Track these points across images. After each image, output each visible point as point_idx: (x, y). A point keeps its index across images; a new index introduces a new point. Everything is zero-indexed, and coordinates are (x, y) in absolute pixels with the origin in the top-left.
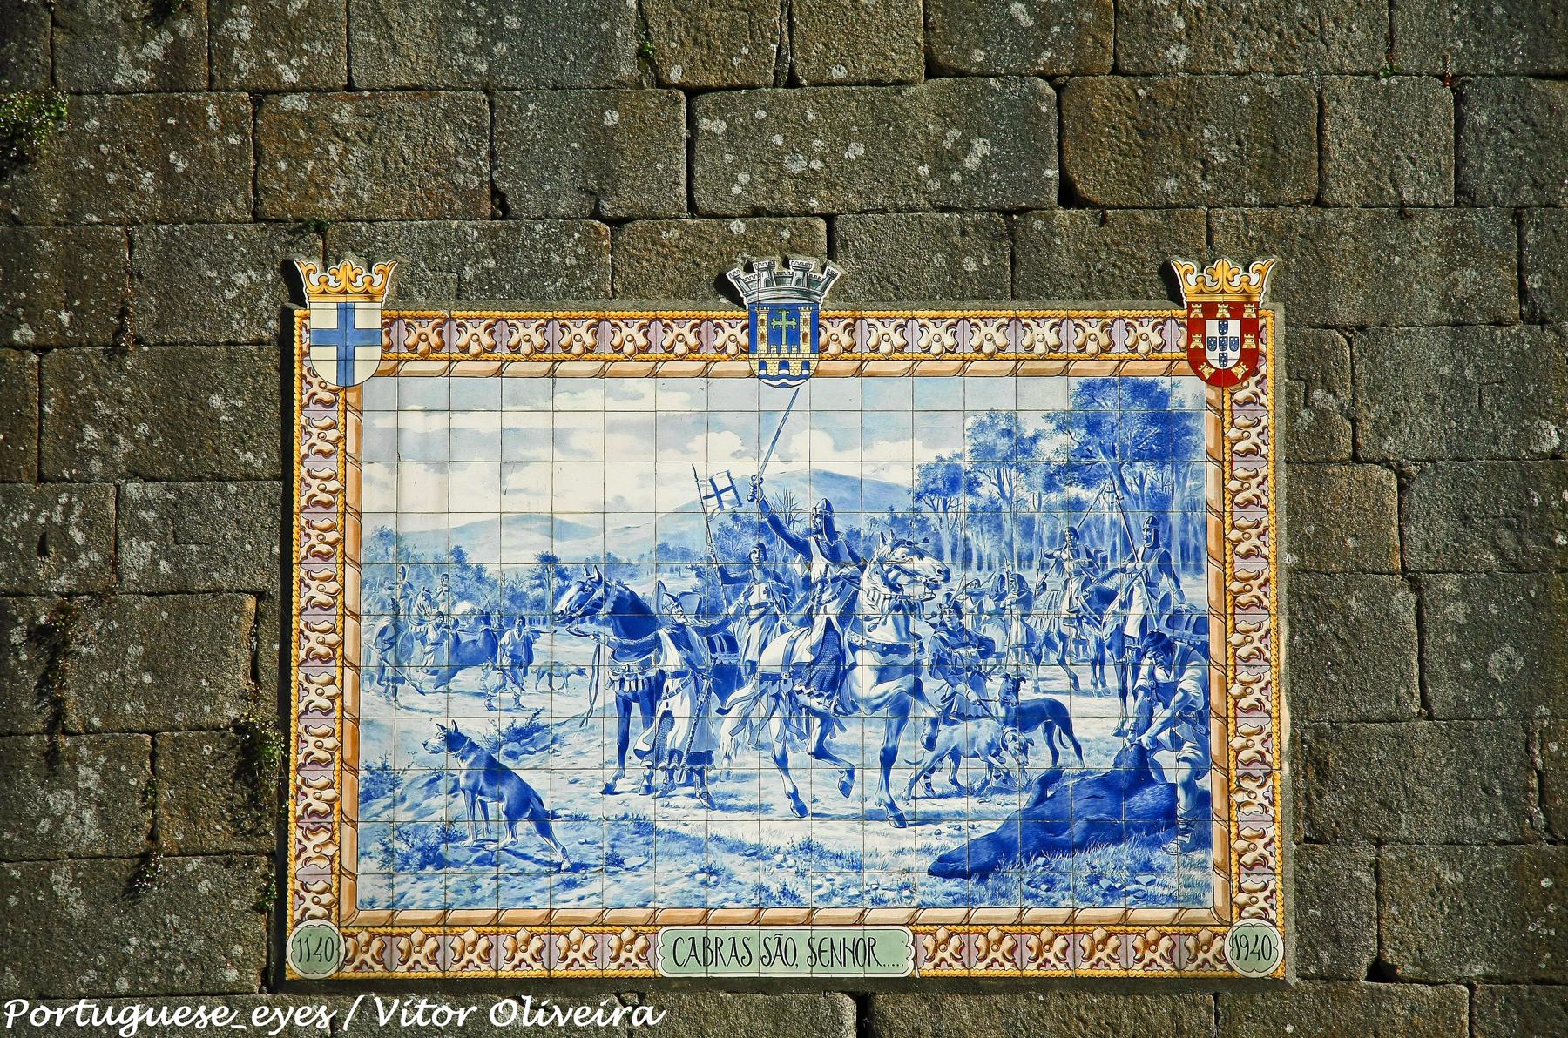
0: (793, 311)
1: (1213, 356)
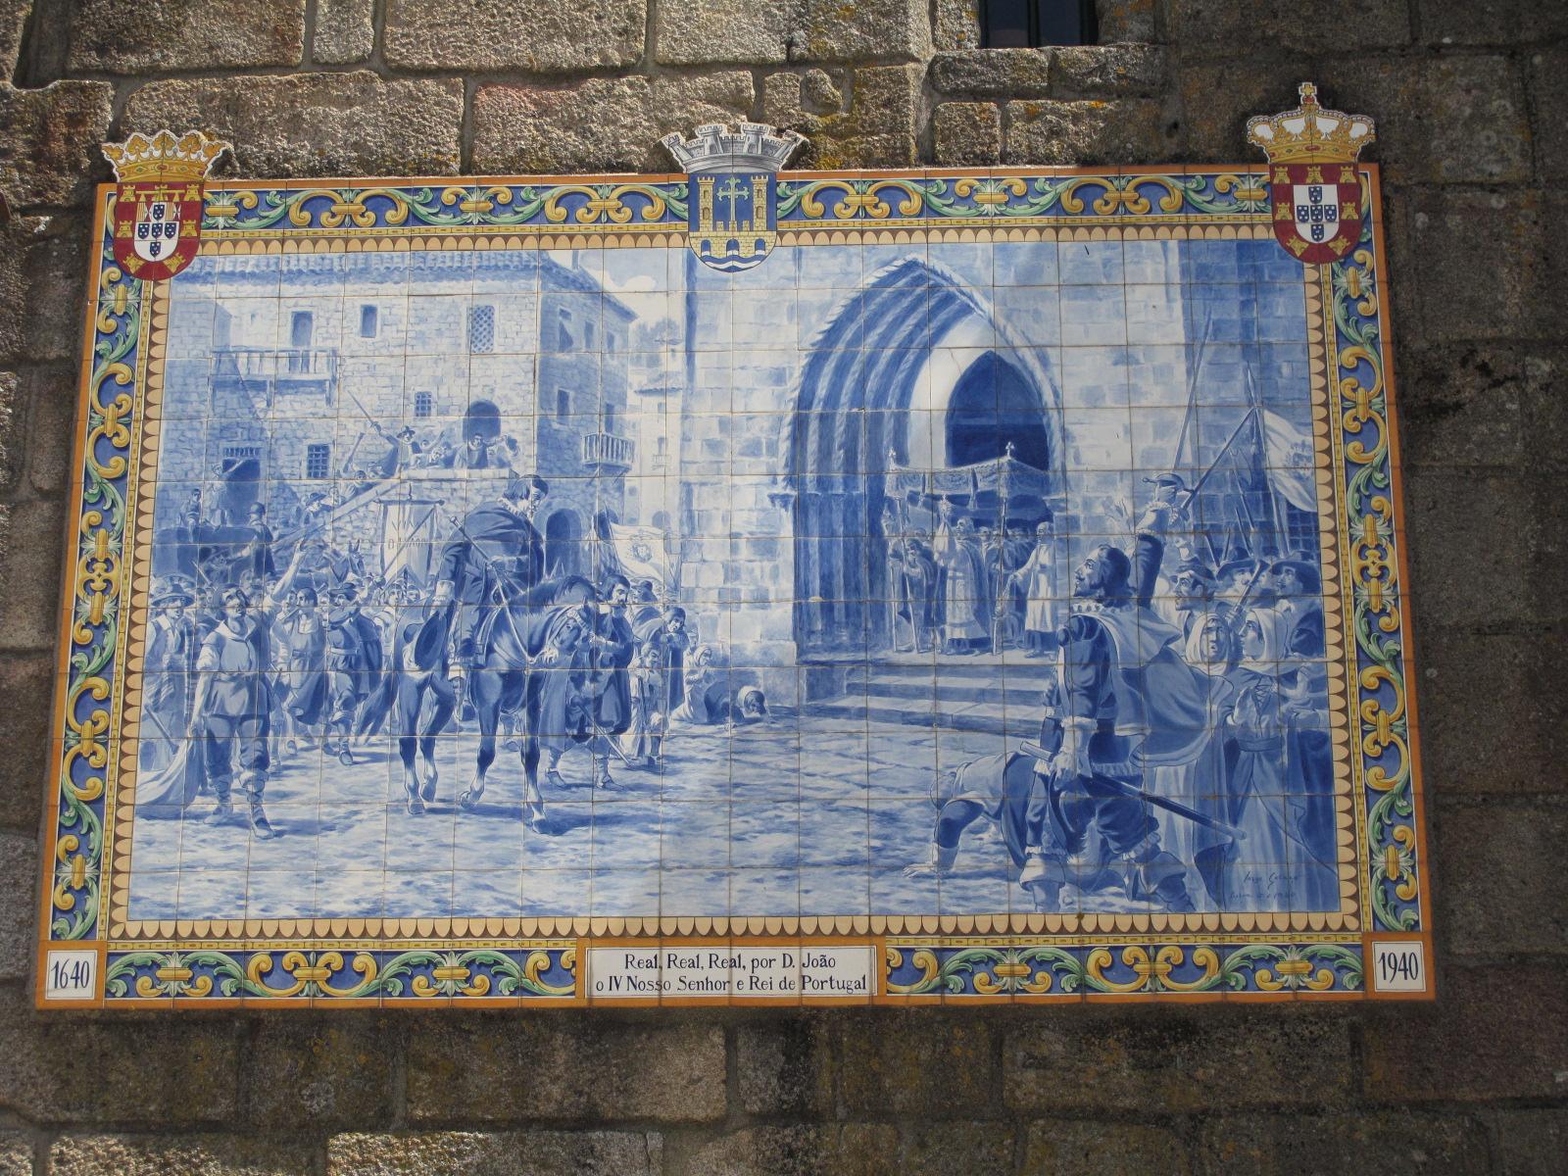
0: (745, 180)
1: (1305, 230)
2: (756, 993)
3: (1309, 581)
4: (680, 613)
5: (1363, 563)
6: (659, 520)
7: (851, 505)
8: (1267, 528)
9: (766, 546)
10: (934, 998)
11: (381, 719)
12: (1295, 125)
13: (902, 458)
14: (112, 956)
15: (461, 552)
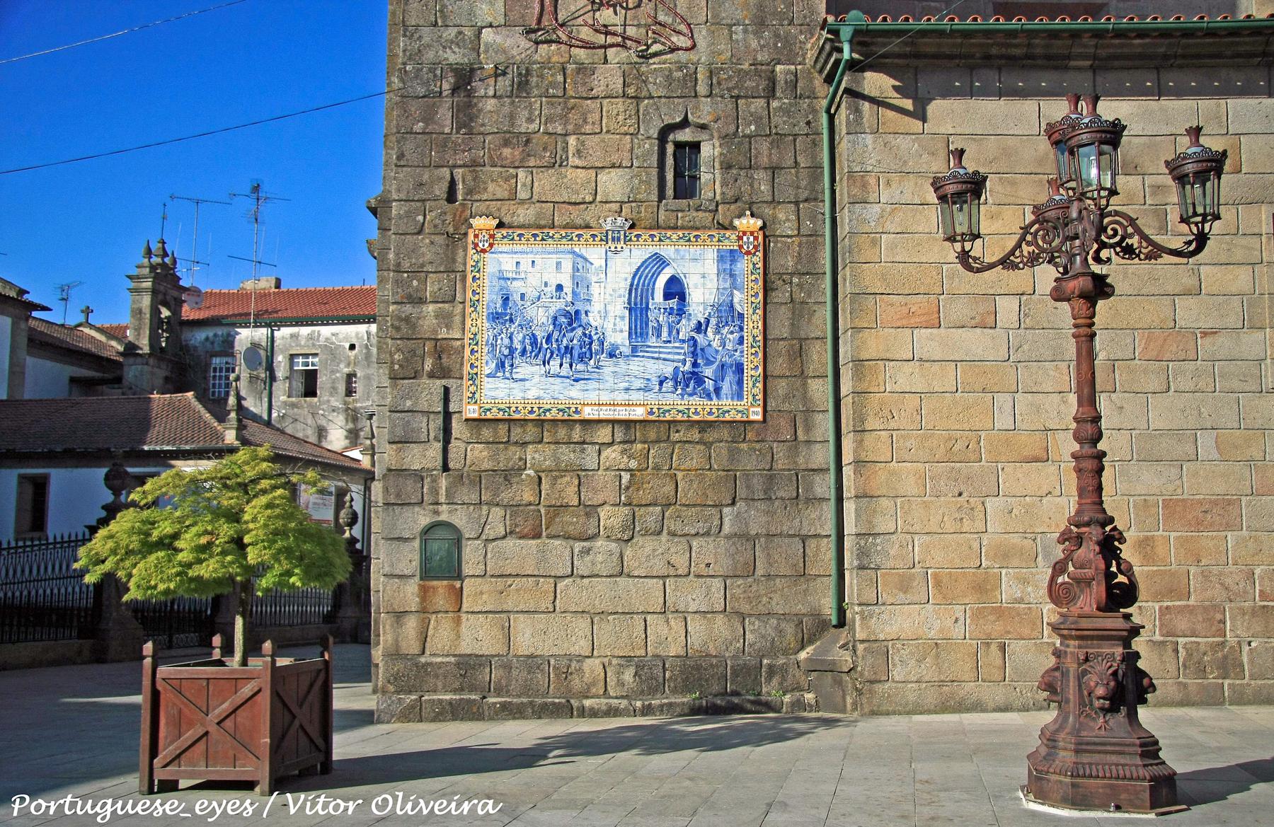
3: (741, 329)
5: (753, 325)
9: (622, 318)
15: (555, 318)
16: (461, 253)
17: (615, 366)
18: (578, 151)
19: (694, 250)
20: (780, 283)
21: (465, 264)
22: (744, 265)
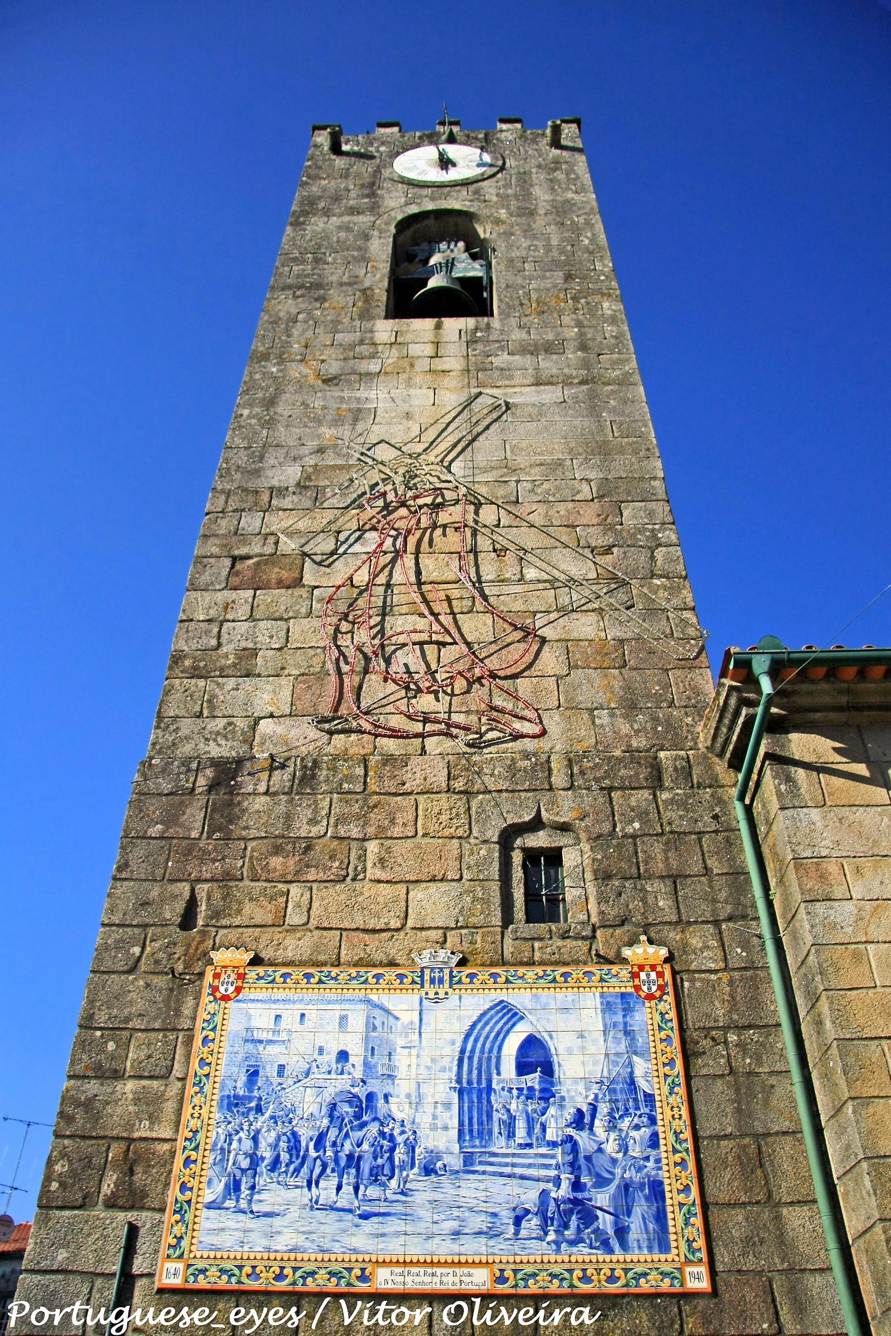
0: (441, 970)
1: (645, 988)
2: (442, 1287)
3: (653, 1120)
4: (415, 1132)
5: (672, 1113)
6: (408, 1096)
7: (480, 1091)
8: (636, 1100)
9: (447, 1106)
10: (513, 1291)
11: (299, 1171)
12: (639, 950)
13: (499, 1074)
14: (189, 1266)
15: (333, 1107)
16: (190, 1001)
17: (435, 1189)
18: (382, 861)
19: (564, 996)
20: (706, 1043)
21: (194, 1019)
22: (644, 1016)
